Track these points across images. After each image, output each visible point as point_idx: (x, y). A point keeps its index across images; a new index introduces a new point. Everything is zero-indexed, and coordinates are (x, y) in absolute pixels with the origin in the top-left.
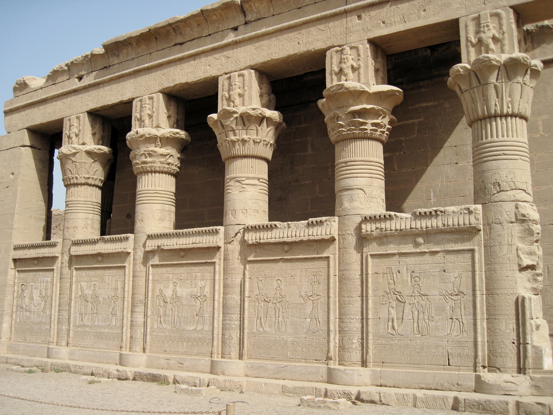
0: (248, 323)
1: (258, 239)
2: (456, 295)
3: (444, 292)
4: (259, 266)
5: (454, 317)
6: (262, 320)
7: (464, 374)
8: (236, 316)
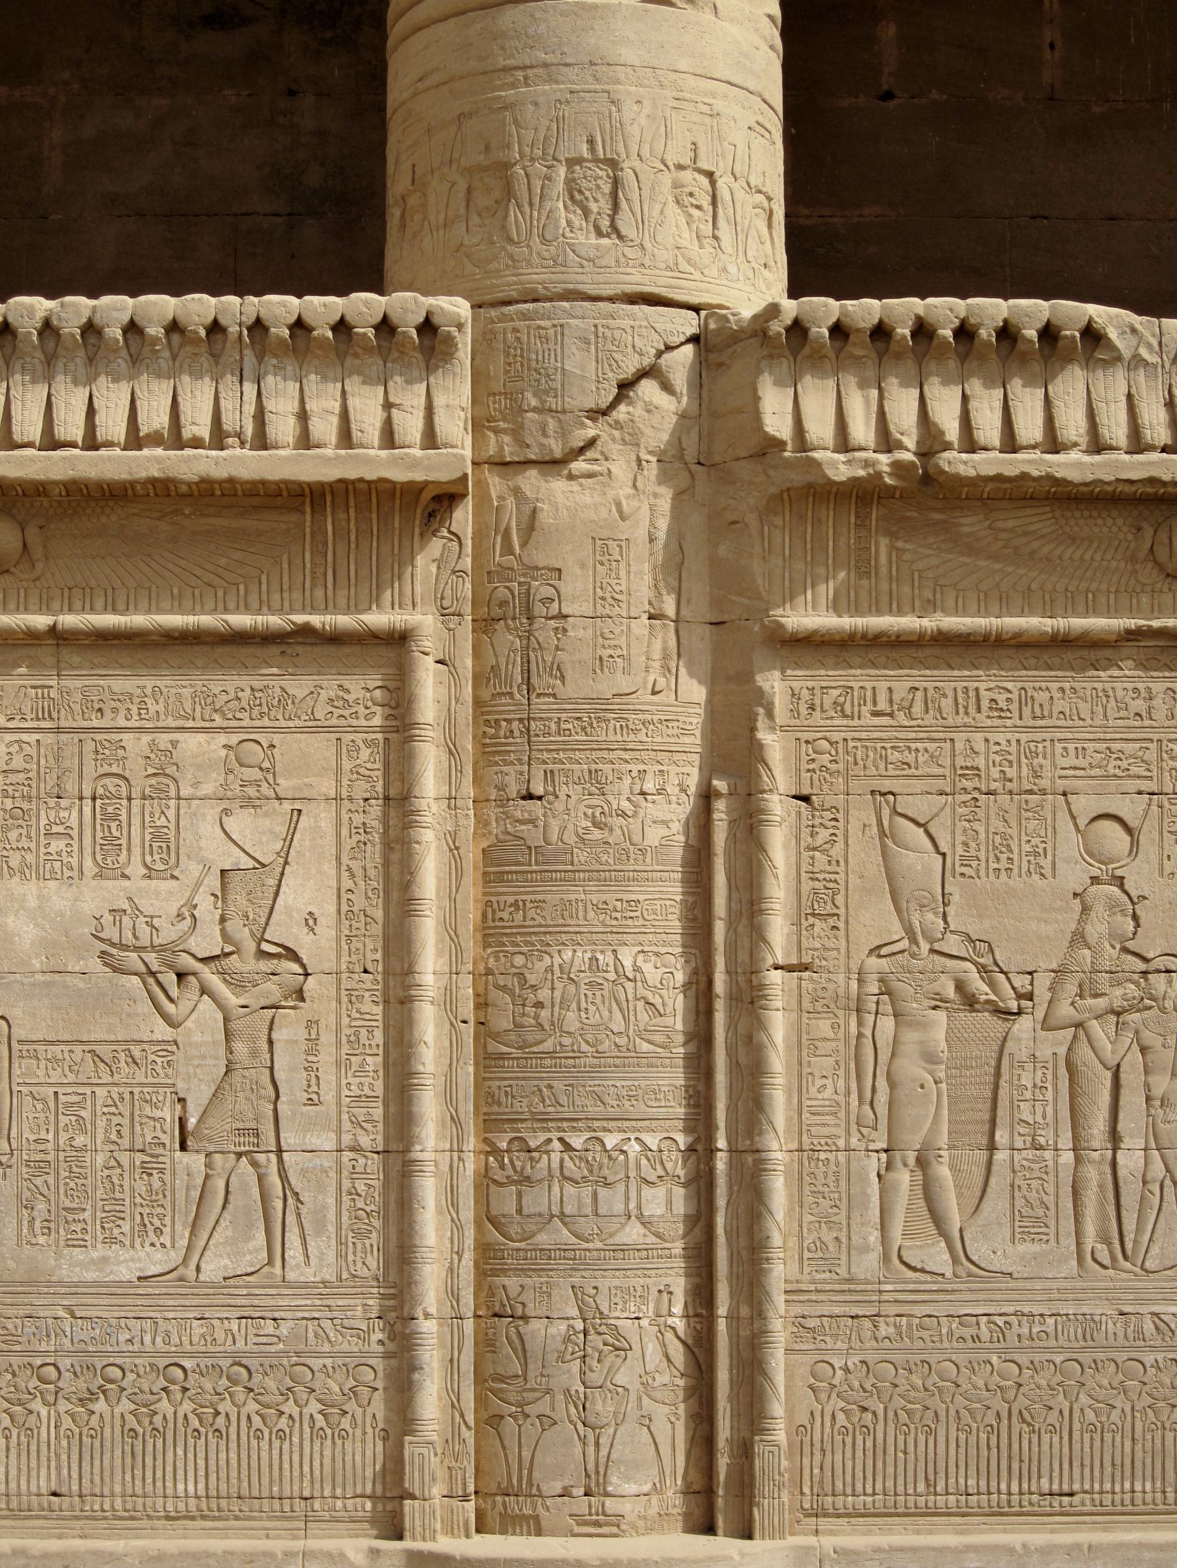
0: (798, 1202)
1: (910, 442)
4: (901, 689)
6: (943, 1171)
8: (652, 1141)
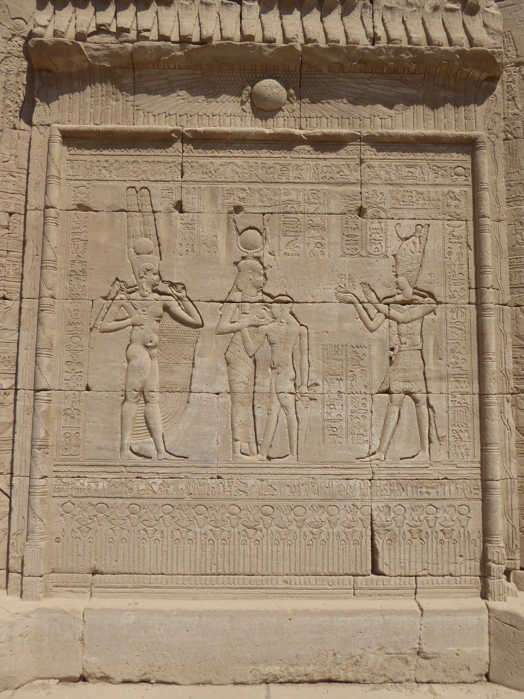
2: (403, 303)
3: (359, 292)
5: (397, 386)
7: (448, 612)
